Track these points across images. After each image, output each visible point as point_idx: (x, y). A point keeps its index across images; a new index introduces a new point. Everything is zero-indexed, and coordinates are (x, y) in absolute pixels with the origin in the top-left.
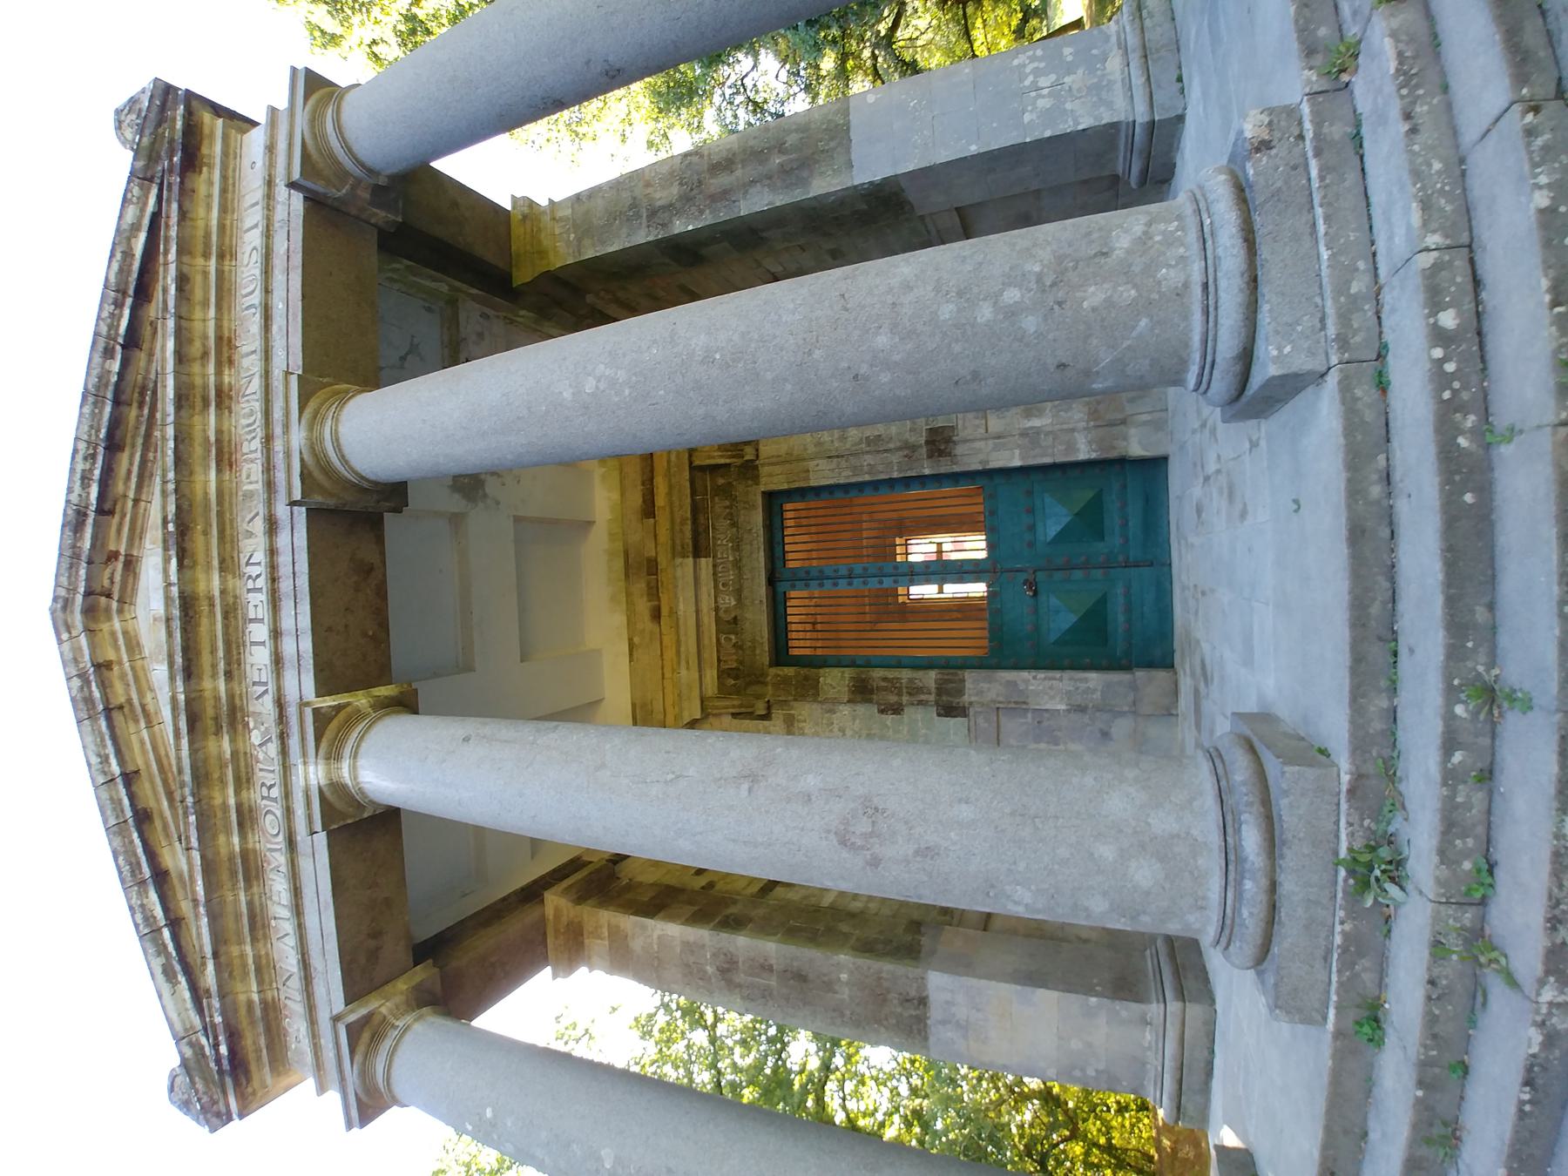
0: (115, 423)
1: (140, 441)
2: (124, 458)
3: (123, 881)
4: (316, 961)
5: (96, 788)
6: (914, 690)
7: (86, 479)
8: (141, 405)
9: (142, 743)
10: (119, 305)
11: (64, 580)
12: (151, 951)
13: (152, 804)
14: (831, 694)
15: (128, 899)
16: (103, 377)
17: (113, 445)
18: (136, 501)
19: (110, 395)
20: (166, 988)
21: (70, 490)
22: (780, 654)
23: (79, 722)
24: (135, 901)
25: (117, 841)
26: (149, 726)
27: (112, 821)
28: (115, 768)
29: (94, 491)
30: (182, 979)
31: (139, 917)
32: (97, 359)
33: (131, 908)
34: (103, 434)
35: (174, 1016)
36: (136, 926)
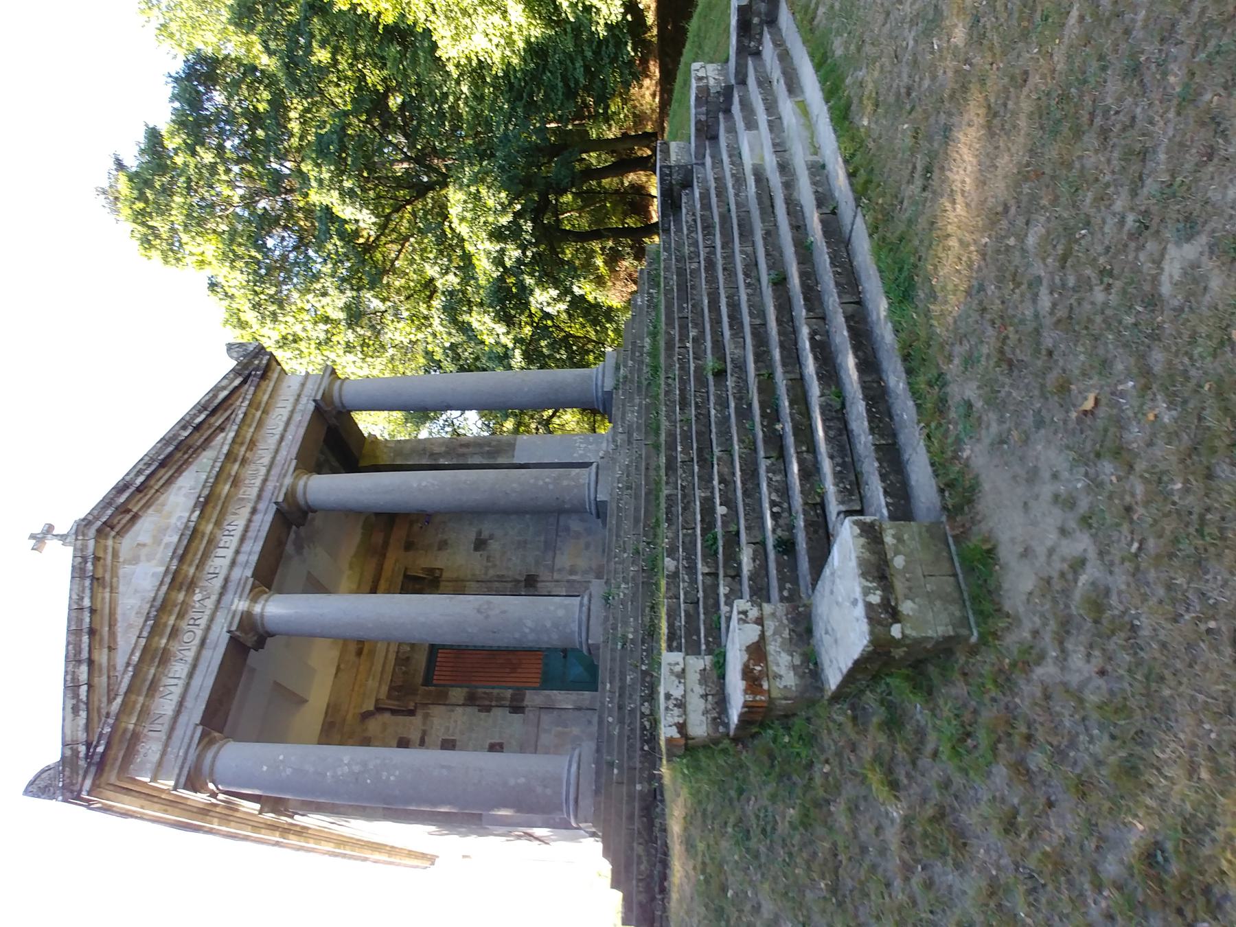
0: (170, 455)
1: (175, 467)
2: (163, 471)
3: (67, 657)
4: (189, 703)
5: (70, 609)
6: (499, 698)
7: (139, 473)
8: (185, 453)
9: (103, 599)
10: (200, 412)
11: (96, 513)
12: (70, 695)
13: (98, 627)
14: (453, 700)
15: (66, 667)
16: (175, 436)
17: (163, 464)
18: (157, 491)
19: (175, 443)
20: (70, 716)
21: (128, 474)
22: (427, 681)
23: (73, 577)
24: (70, 668)
25: (72, 638)
26: (111, 592)
27: (74, 627)
28: (87, 602)
29: (141, 479)
30: (83, 714)
31: (69, 678)
32: (177, 428)
33: (66, 672)
34: (162, 457)
35: (68, 732)
36: (65, 681)
